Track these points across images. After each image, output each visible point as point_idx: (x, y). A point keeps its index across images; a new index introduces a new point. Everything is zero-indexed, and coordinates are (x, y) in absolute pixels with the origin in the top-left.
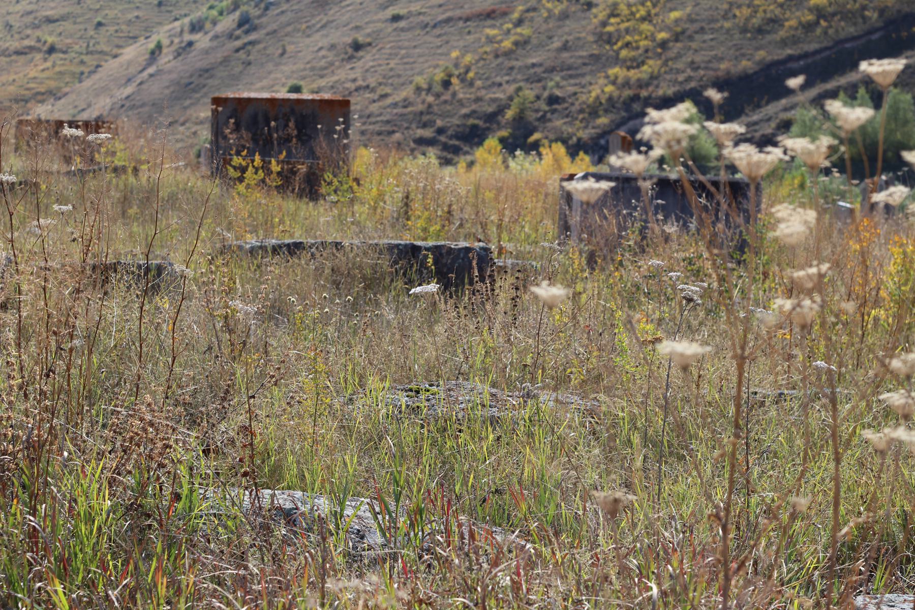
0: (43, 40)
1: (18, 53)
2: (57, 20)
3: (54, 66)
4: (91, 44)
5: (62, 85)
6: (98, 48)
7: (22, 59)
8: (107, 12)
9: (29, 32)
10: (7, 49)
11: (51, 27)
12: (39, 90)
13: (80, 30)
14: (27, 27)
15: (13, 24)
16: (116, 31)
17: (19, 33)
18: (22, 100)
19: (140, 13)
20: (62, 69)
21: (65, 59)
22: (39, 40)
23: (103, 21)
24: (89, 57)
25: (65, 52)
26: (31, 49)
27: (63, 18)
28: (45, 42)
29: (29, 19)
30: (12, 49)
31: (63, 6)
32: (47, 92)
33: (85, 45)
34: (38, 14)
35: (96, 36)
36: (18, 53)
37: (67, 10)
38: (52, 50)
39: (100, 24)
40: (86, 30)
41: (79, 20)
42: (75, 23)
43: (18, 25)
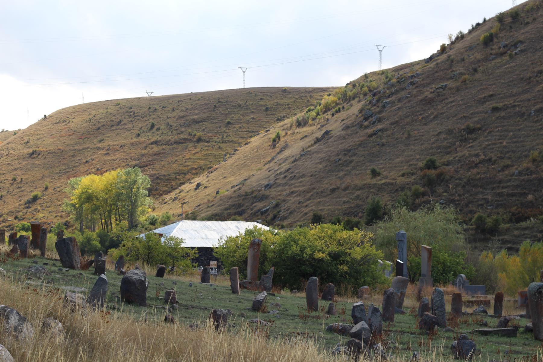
0: (193, 134)
1: (176, 143)
2: (201, 121)
3: (201, 151)
4: (225, 136)
5: (208, 163)
6: (230, 138)
7: (180, 146)
8: (233, 115)
9: (183, 129)
10: (170, 140)
11: (197, 126)
12: (193, 167)
13: (216, 128)
14: (181, 126)
15: (172, 124)
16: (241, 127)
17: (176, 130)
18: (182, 173)
19: (255, 116)
20: (207, 152)
21: (209, 146)
22: (190, 134)
23: (231, 121)
24: (224, 144)
25: (207, 142)
26: (185, 139)
27: (204, 120)
28: (195, 135)
29: (182, 121)
30: (173, 140)
31: (204, 113)
32: (198, 167)
33: (221, 137)
34: (188, 118)
35: (228, 131)
36: (176, 143)
37: (206, 115)
38: (199, 140)
39: (229, 123)
40: (220, 127)
41: (215, 121)
42: (212, 123)
43: (175, 125)
